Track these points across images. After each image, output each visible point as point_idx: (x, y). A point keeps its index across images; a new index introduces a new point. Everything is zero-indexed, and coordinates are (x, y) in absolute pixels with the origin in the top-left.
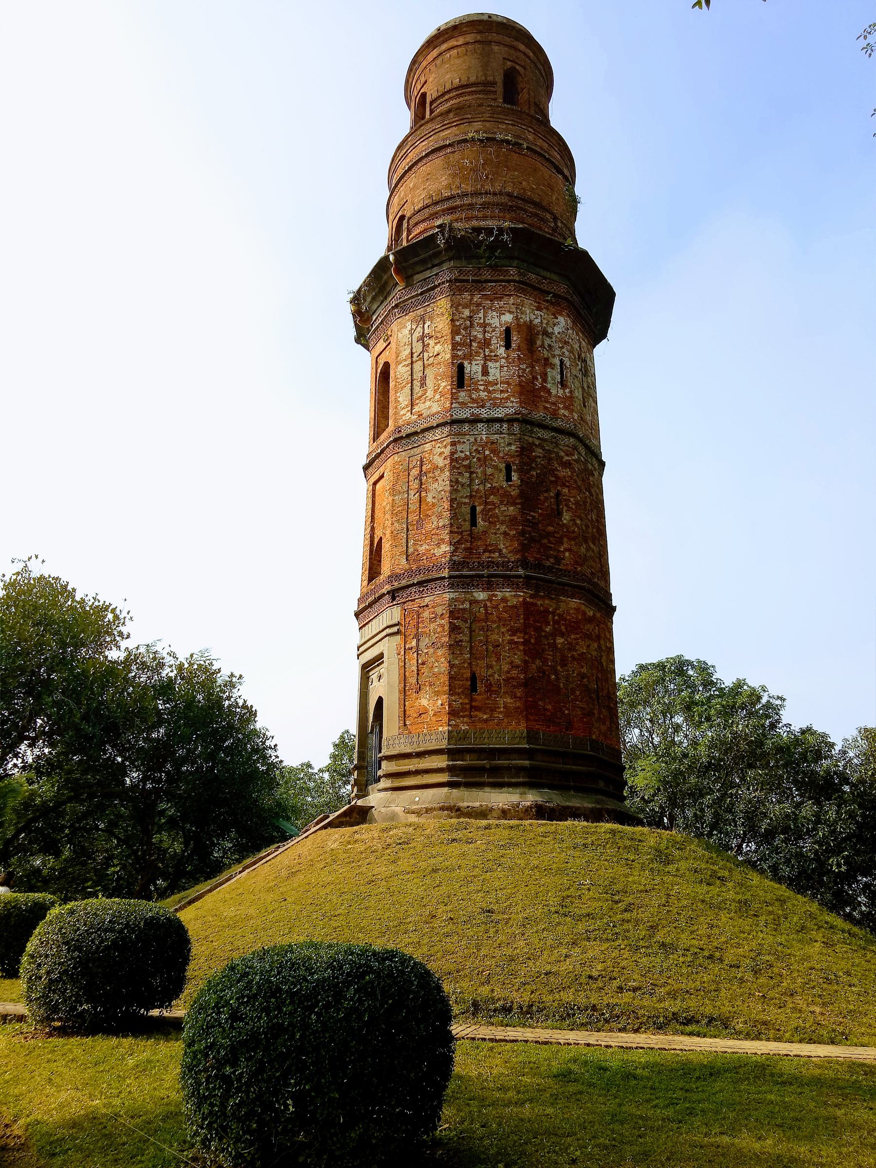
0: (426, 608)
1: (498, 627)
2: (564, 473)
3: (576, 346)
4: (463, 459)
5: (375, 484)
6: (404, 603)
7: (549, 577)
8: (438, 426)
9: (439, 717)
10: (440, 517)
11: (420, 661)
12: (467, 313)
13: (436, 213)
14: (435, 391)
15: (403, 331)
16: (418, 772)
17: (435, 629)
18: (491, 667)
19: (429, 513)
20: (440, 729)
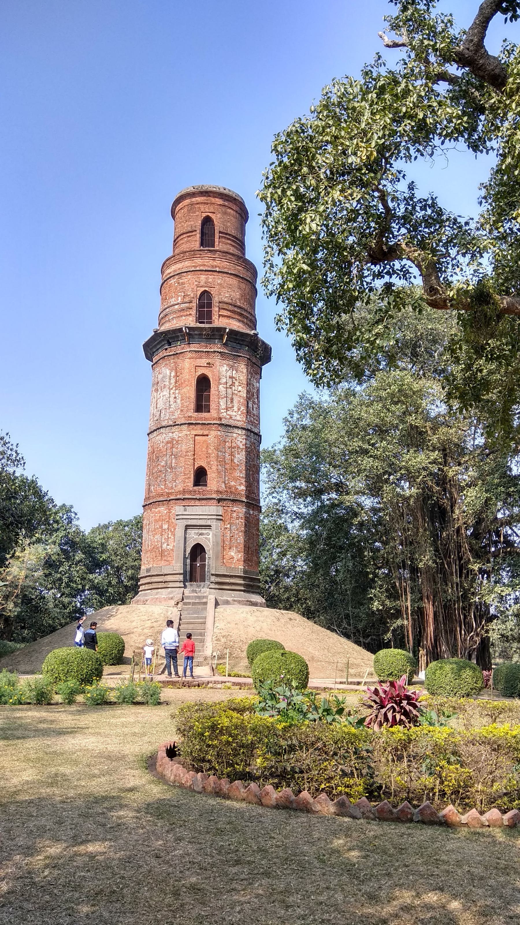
5: (196, 435)
8: (242, 428)
10: (241, 472)
13: (235, 311)
14: (239, 409)
19: (236, 468)
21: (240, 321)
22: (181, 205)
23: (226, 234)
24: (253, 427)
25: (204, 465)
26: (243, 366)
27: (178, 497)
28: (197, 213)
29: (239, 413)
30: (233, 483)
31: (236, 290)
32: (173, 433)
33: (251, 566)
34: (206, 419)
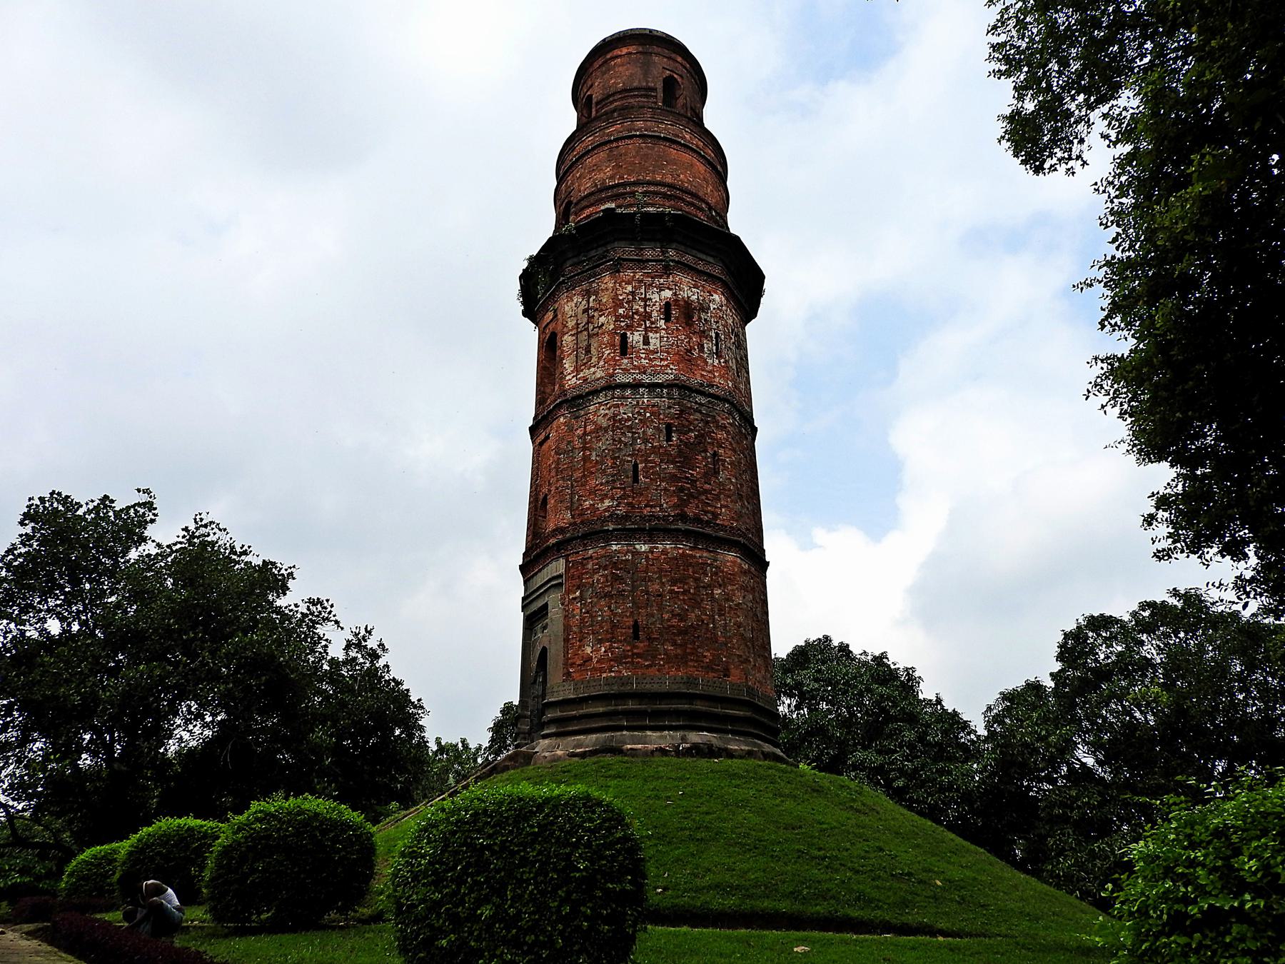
1: (660, 578)
2: (721, 435)
3: (730, 322)
4: (627, 420)
5: (541, 444)
7: (708, 531)
8: (603, 389)
12: (629, 288)
14: (600, 358)
15: (570, 306)
18: (653, 615)
23: (609, 96)
29: (602, 363)
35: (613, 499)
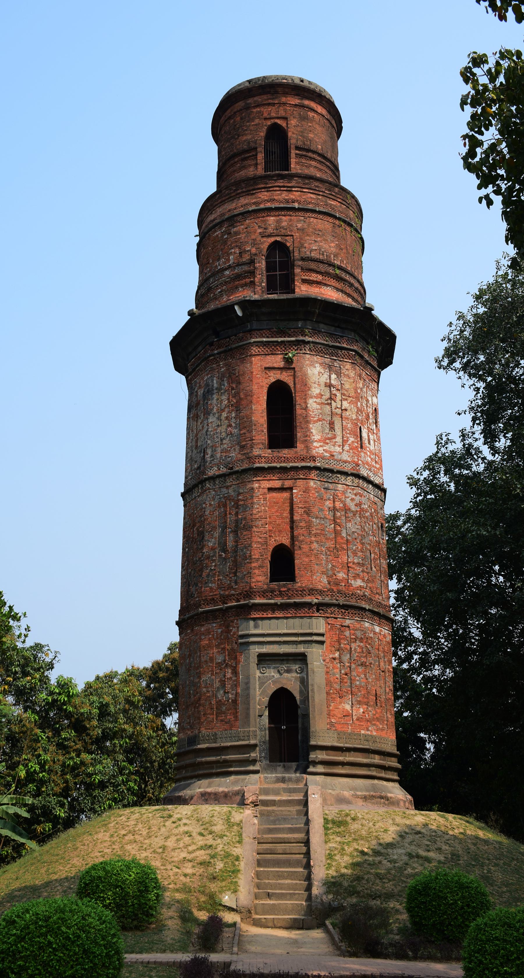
0: (347, 629)
5: (270, 489)
6: (328, 618)
8: (353, 475)
9: (360, 721)
11: (343, 672)
16: (343, 764)
17: (355, 649)
19: (345, 546)
20: (363, 732)
21: (338, 289)
22: (228, 113)
23: (308, 150)
24: (371, 474)
25: (286, 541)
26: (348, 366)
27: (242, 602)
28: (257, 121)
29: (347, 448)
30: (341, 575)
31: (330, 238)
32: (227, 487)
33: (382, 730)
34: (287, 460)
35: (363, 580)
